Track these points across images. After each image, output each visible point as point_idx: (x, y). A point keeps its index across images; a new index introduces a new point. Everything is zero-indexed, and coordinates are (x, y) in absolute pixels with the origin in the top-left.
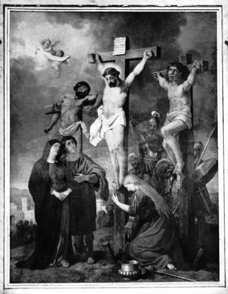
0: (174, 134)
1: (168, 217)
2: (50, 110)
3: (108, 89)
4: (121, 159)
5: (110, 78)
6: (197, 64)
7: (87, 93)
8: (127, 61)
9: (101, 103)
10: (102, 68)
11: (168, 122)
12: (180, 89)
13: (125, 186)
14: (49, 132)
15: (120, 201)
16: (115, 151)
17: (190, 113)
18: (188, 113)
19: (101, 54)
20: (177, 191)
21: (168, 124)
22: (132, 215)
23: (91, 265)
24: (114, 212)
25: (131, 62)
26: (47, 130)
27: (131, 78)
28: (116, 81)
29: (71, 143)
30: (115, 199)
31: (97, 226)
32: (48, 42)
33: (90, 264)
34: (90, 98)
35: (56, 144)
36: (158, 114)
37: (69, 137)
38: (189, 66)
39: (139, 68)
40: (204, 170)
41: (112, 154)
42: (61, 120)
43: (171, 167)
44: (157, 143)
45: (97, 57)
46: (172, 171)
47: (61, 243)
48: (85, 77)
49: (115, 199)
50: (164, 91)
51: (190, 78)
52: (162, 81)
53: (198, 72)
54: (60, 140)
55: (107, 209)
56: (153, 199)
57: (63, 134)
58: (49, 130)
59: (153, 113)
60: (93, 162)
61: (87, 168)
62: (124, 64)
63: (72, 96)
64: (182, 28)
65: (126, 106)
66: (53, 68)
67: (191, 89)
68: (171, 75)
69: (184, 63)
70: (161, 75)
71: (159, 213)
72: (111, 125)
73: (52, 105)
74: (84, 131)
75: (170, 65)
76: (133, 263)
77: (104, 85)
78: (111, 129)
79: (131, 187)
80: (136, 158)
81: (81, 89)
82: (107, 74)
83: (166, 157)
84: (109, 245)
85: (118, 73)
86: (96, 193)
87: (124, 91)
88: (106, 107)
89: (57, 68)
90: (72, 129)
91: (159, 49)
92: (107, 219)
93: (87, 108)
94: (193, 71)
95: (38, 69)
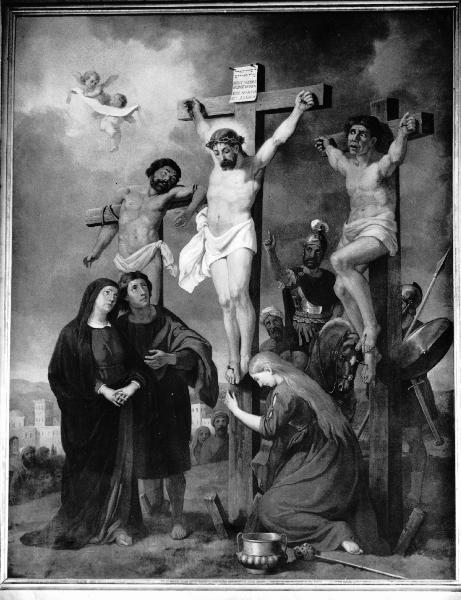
0: (359, 268)
1: (344, 439)
2: (97, 218)
3: (218, 174)
4: (244, 319)
5: (223, 151)
6: (408, 119)
8: (260, 115)
9: (204, 202)
10: (207, 130)
11: (347, 242)
12: (372, 172)
13: (253, 376)
14: (94, 263)
15: (242, 407)
16: (231, 304)
17: (395, 223)
18: (390, 224)
20: (365, 386)
21: (345, 246)
22: (268, 437)
23: (177, 542)
24: (229, 431)
25: (269, 117)
26: (89, 259)
27: (268, 148)
28: (235, 157)
30: (232, 404)
31: (193, 459)
32: (92, 78)
33: (176, 539)
34: (180, 192)
35: (108, 288)
36: (326, 225)
37: (135, 275)
38: (392, 124)
39: (284, 130)
40: (425, 343)
41: (225, 310)
42: (119, 240)
43: (351, 336)
44: (321, 288)
45: (196, 108)
46: (355, 344)
47: (116, 497)
48: (166, 148)
49: (232, 404)
51: (395, 149)
52: (334, 155)
53: (411, 136)
54: (117, 281)
56: (314, 405)
57: (122, 268)
58: (93, 259)
59: (314, 223)
60: (185, 327)
61: (173, 338)
62: (254, 120)
63: (145, 186)
64: (378, 45)
65: (256, 210)
66: (104, 131)
67: (397, 172)
68: (354, 144)
69: (382, 117)
70: (332, 143)
71: (326, 432)
73: (100, 209)
74: (168, 262)
75: (351, 123)
76: (269, 537)
77: (211, 165)
78: (225, 258)
79: (265, 378)
80: (277, 318)
82: (217, 143)
83: (340, 316)
85: (241, 140)
86: (191, 391)
87: (253, 177)
88: (214, 209)
89: (111, 130)
90: (145, 254)
91: (328, 90)
92: (215, 445)
93: (172, 214)
94: (400, 135)
95: (72, 133)
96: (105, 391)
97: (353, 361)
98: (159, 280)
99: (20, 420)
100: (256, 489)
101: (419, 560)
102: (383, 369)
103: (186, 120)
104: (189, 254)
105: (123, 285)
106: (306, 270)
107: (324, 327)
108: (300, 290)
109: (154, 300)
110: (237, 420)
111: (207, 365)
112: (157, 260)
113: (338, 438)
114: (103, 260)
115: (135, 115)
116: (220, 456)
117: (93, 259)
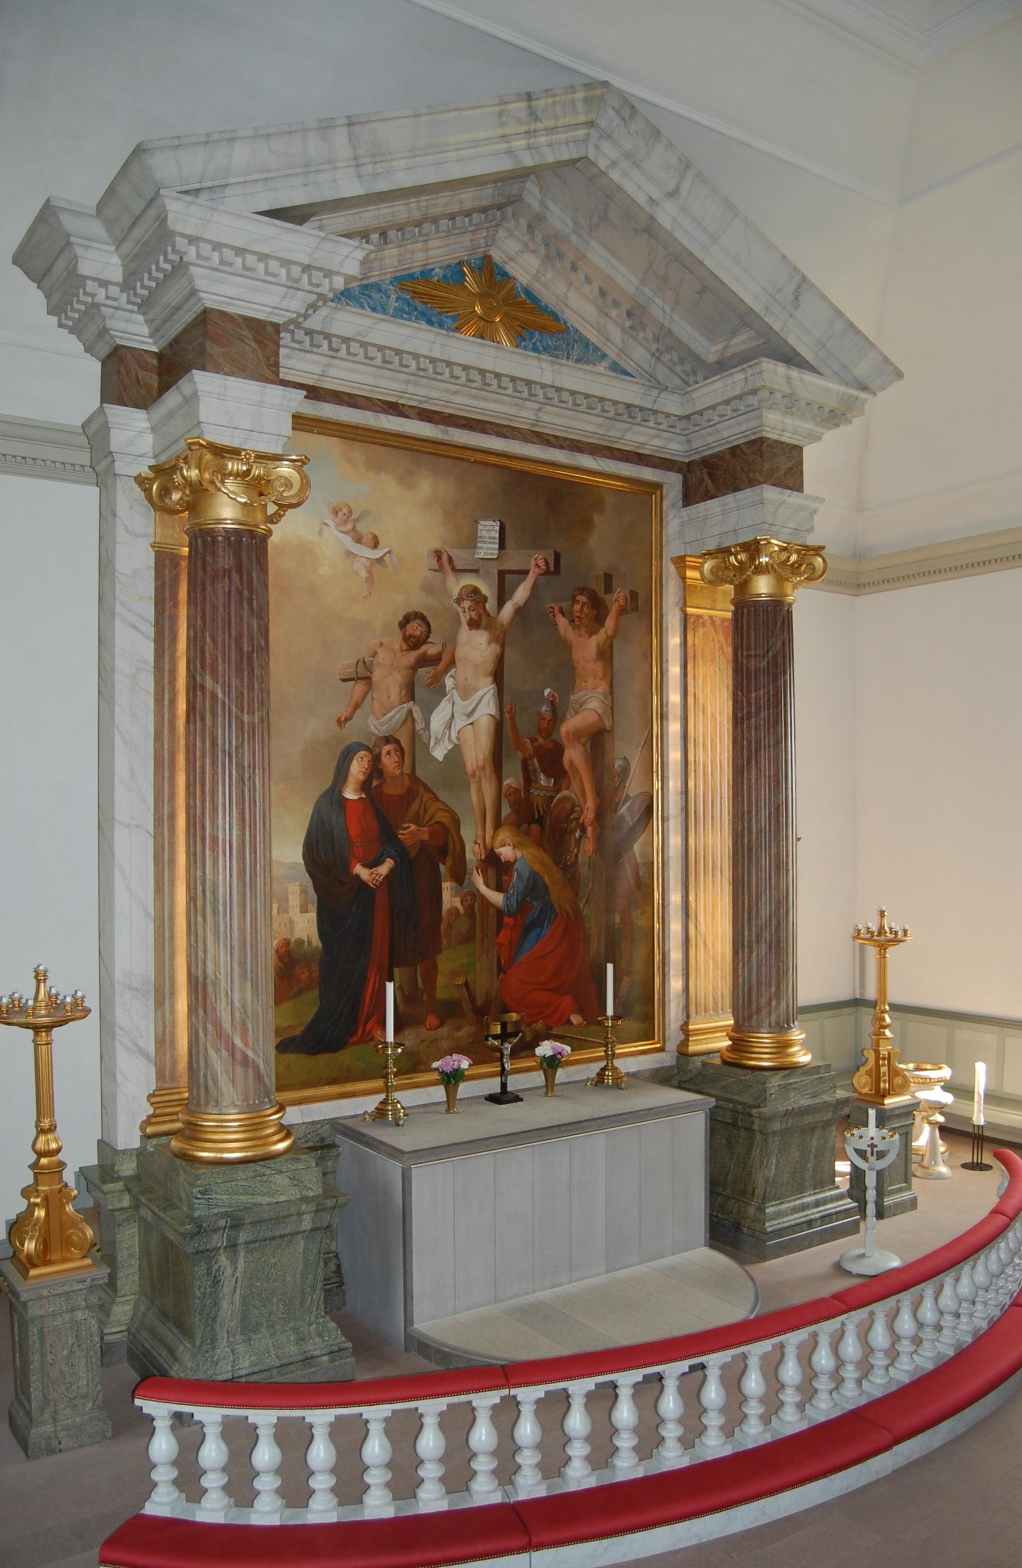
0: (583, 740)
2: (350, 672)
3: (464, 633)
8: (502, 574)
9: (452, 663)
10: (456, 585)
13: (497, 851)
14: (348, 724)
15: (487, 884)
16: (477, 774)
17: (610, 697)
18: (606, 697)
19: (453, 553)
21: (572, 717)
22: (510, 915)
23: (432, 1033)
24: (476, 910)
25: (508, 577)
26: (343, 719)
27: (508, 609)
28: (480, 616)
29: (393, 753)
31: (444, 941)
32: (345, 510)
33: (430, 1029)
34: (431, 650)
35: (362, 753)
37: (388, 740)
39: (521, 594)
41: (472, 780)
42: (373, 698)
44: (551, 759)
45: (445, 558)
47: (374, 987)
48: (418, 601)
50: (565, 646)
51: (610, 622)
52: (562, 622)
53: (622, 611)
54: (371, 745)
55: (462, 904)
56: (547, 879)
57: (376, 732)
58: (347, 720)
59: (547, 692)
61: (426, 810)
64: (597, 518)
65: (498, 676)
66: (357, 573)
67: (611, 646)
69: (600, 591)
72: (470, 715)
73: (353, 661)
74: (419, 726)
76: (512, 1017)
77: (459, 623)
78: (472, 724)
79: (506, 852)
80: (517, 790)
81: (415, 630)
83: (568, 788)
84: (466, 984)
85: (485, 599)
86: (442, 868)
88: (463, 671)
89: (364, 574)
90: (397, 716)
91: (557, 556)
92: (463, 926)
95: (324, 570)
97: (578, 834)
98: (409, 743)
100: (500, 970)
103: (435, 571)
104: (437, 720)
105: (377, 750)
106: (541, 740)
107: (555, 800)
108: (535, 760)
109: (407, 768)
110: (483, 897)
111: (456, 839)
112: (409, 723)
113: (567, 913)
114: (357, 721)
115: (387, 558)
116: (468, 938)
117: (347, 720)
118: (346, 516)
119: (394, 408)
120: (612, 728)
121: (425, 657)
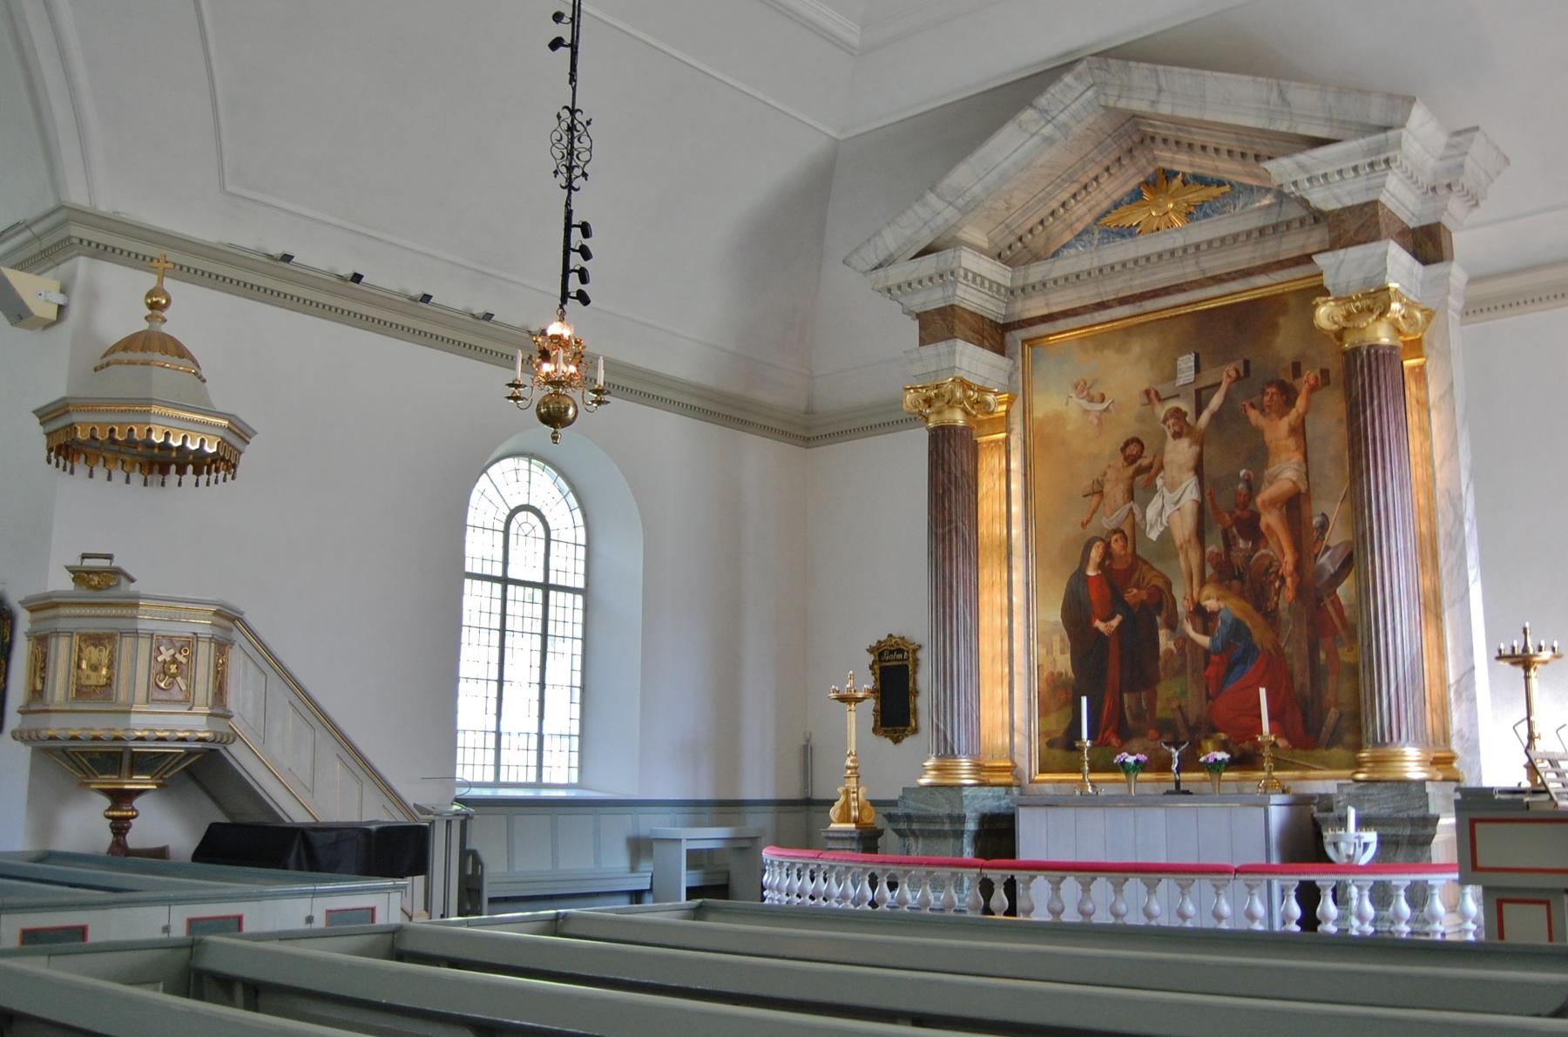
4: (1194, 557)
7: (1139, 456)
8: (1198, 392)
9: (1161, 467)
10: (1162, 411)
12: (1284, 424)
15: (1195, 629)
19: (1159, 388)
25: (1204, 393)
27: (1205, 416)
30: (1189, 629)
34: (1144, 462)
37: (1115, 531)
38: (1297, 383)
39: (1216, 401)
40: (1333, 564)
44: (1250, 527)
49: (1189, 629)
50: (1258, 432)
51: (1300, 403)
52: (1254, 415)
60: (1152, 568)
63: (1120, 461)
64: (1282, 321)
65: (1198, 469)
69: (1288, 379)
70: (1253, 406)
74: (1138, 518)
77: (1165, 436)
79: (1211, 604)
80: (1218, 555)
81: (1132, 450)
84: (1180, 707)
85: (1185, 414)
86: (1158, 619)
88: (1170, 472)
89: (1095, 421)
91: (1247, 363)
93: (1140, 479)
95: (1070, 427)
96: (1099, 624)
98: (1131, 532)
99: (1043, 651)
100: (1209, 697)
101: (1337, 752)
102: (1300, 590)
104: (1151, 512)
106: (1238, 512)
109: (1129, 550)
110: (1192, 640)
114: (1094, 522)
116: (1181, 671)
118: (1084, 389)
119: (1102, 306)
120: (1308, 490)
121: (1140, 465)
